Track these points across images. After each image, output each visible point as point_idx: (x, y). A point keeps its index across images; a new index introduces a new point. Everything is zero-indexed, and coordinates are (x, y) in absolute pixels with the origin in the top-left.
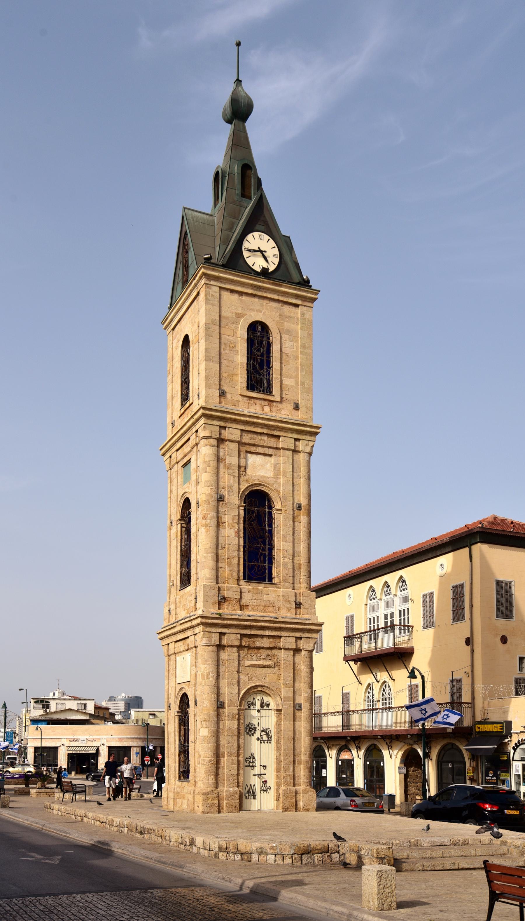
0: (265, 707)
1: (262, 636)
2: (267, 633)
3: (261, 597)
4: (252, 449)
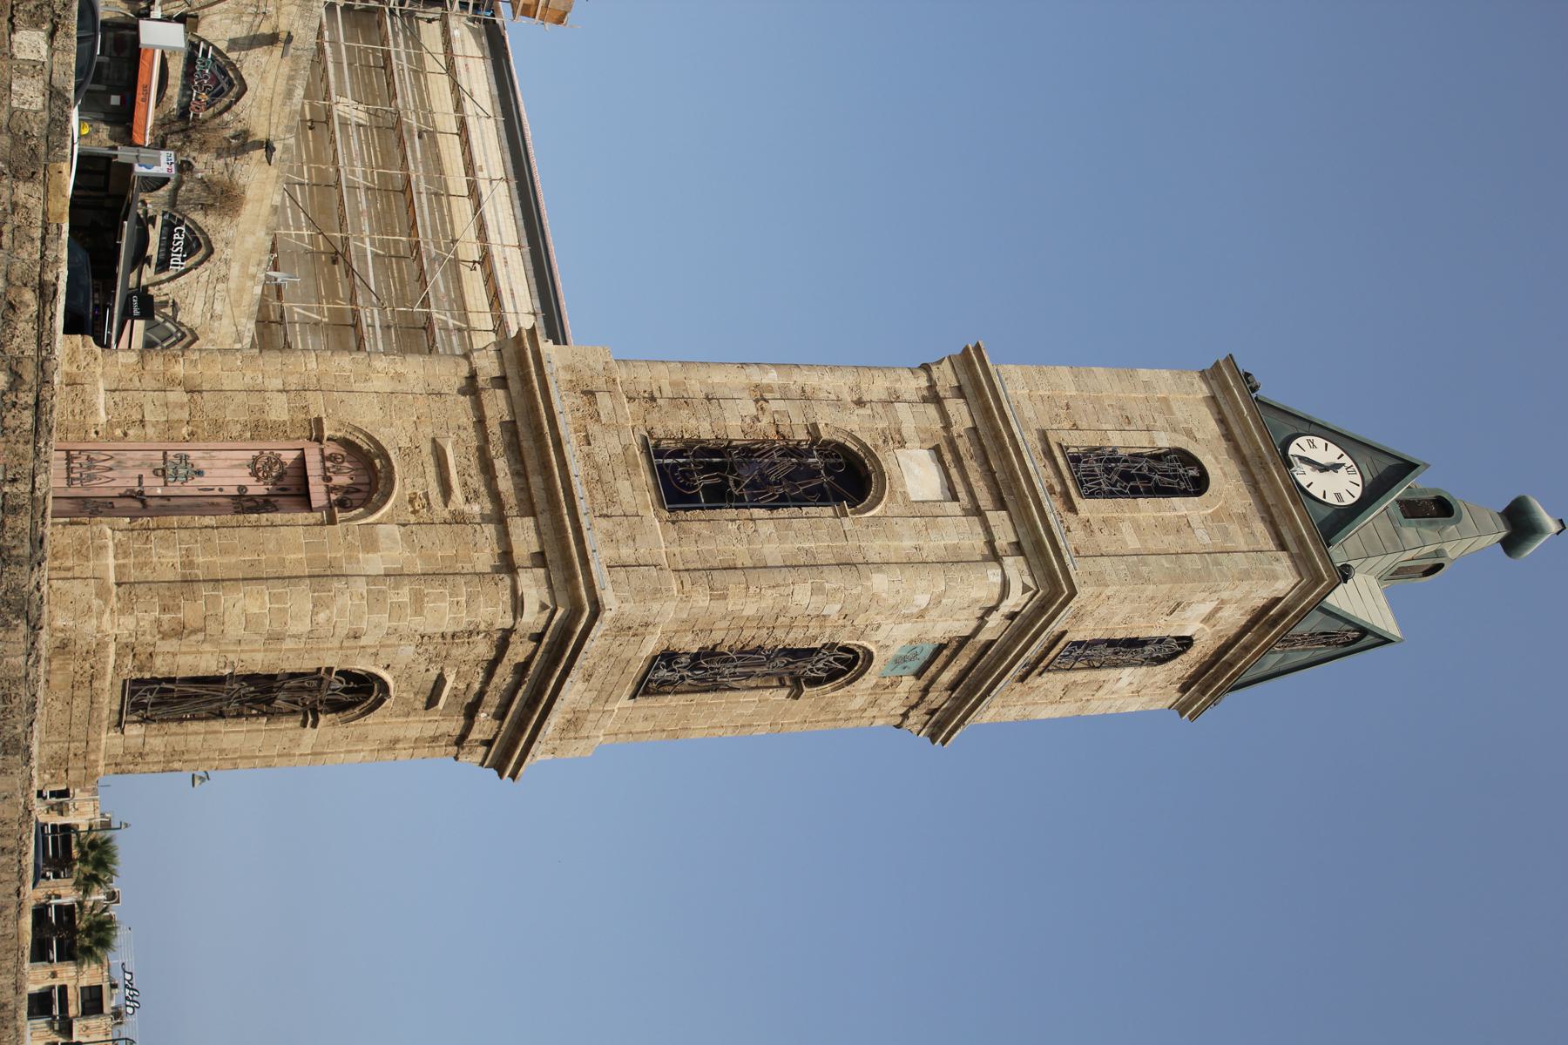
0: (333, 497)
1: (520, 474)
2: (536, 481)
3: (620, 470)
4: (948, 457)
